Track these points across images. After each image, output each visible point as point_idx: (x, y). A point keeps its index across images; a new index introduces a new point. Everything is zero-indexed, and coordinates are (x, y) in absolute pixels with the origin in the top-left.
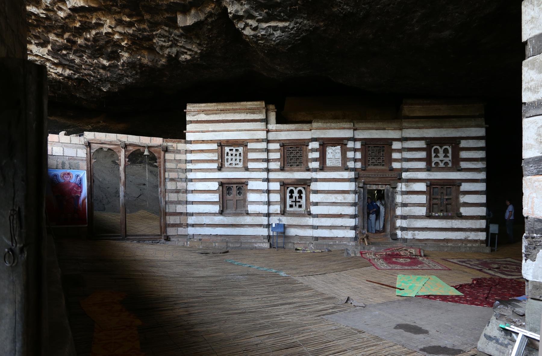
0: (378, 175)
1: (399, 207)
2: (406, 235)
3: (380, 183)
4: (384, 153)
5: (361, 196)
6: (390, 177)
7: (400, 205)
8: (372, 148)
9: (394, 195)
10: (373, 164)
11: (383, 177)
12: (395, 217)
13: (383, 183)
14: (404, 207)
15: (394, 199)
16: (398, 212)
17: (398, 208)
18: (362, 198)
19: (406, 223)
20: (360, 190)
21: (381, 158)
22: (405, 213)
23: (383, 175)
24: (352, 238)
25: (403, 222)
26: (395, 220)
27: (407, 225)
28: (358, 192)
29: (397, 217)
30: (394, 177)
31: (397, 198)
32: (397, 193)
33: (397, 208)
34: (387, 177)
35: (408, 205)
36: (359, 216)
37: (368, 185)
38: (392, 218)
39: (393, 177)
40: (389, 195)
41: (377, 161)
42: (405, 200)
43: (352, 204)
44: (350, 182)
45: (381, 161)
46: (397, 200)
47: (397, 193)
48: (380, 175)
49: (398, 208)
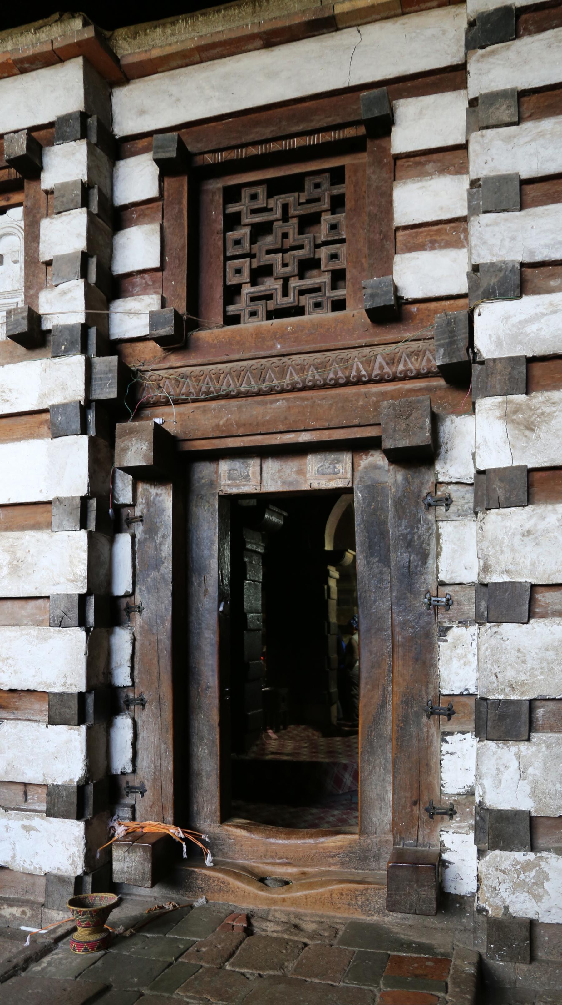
0: (283, 372)
1: (464, 623)
2: (517, 886)
3: (305, 437)
4: (341, 217)
5: (158, 548)
6: (381, 380)
7: (469, 609)
8: (254, 197)
9: (415, 522)
10: (260, 307)
11: (325, 386)
12: (432, 712)
13: (325, 436)
14: (499, 622)
15: (424, 557)
16: (455, 663)
17: (456, 632)
18: (167, 567)
19: (522, 776)
20: (149, 504)
21: (323, 253)
22: (510, 674)
23: (321, 366)
24: (61, 880)
25: (489, 766)
26: (436, 737)
27: (533, 795)
28: (141, 519)
29: (450, 713)
30: (419, 376)
31: (446, 547)
32: (448, 501)
33: (445, 631)
34: (359, 382)
35: (544, 597)
36: (143, 703)
37: (224, 466)
38: (405, 720)
39: (405, 378)
40: (384, 534)
41: (294, 283)
42: (506, 558)
43: (63, 605)
44: (55, 436)
45: (326, 278)
46: (443, 563)
47: (448, 501)
48: (302, 369)
49: (456, 632)
